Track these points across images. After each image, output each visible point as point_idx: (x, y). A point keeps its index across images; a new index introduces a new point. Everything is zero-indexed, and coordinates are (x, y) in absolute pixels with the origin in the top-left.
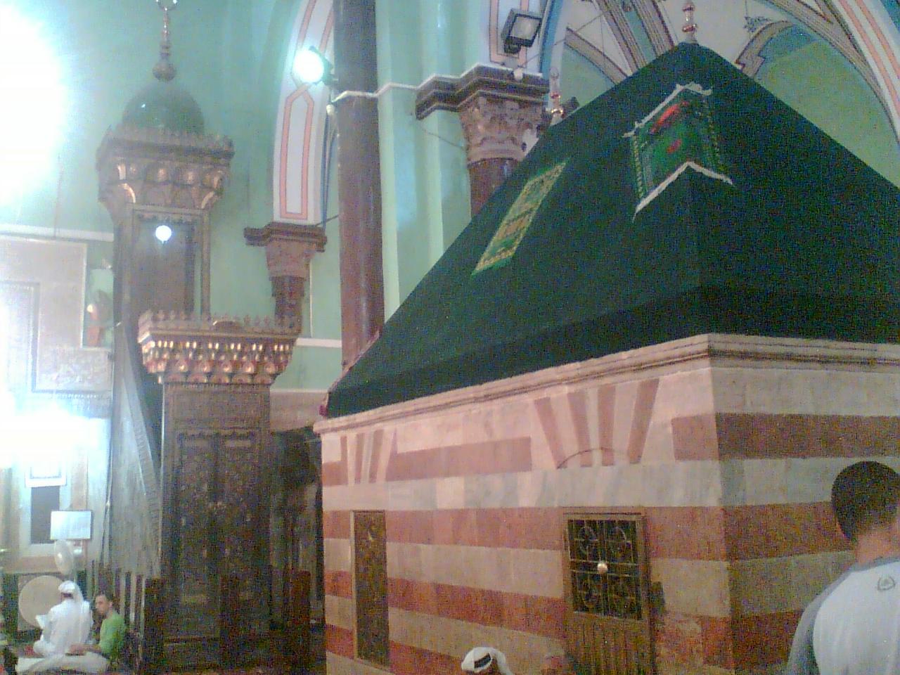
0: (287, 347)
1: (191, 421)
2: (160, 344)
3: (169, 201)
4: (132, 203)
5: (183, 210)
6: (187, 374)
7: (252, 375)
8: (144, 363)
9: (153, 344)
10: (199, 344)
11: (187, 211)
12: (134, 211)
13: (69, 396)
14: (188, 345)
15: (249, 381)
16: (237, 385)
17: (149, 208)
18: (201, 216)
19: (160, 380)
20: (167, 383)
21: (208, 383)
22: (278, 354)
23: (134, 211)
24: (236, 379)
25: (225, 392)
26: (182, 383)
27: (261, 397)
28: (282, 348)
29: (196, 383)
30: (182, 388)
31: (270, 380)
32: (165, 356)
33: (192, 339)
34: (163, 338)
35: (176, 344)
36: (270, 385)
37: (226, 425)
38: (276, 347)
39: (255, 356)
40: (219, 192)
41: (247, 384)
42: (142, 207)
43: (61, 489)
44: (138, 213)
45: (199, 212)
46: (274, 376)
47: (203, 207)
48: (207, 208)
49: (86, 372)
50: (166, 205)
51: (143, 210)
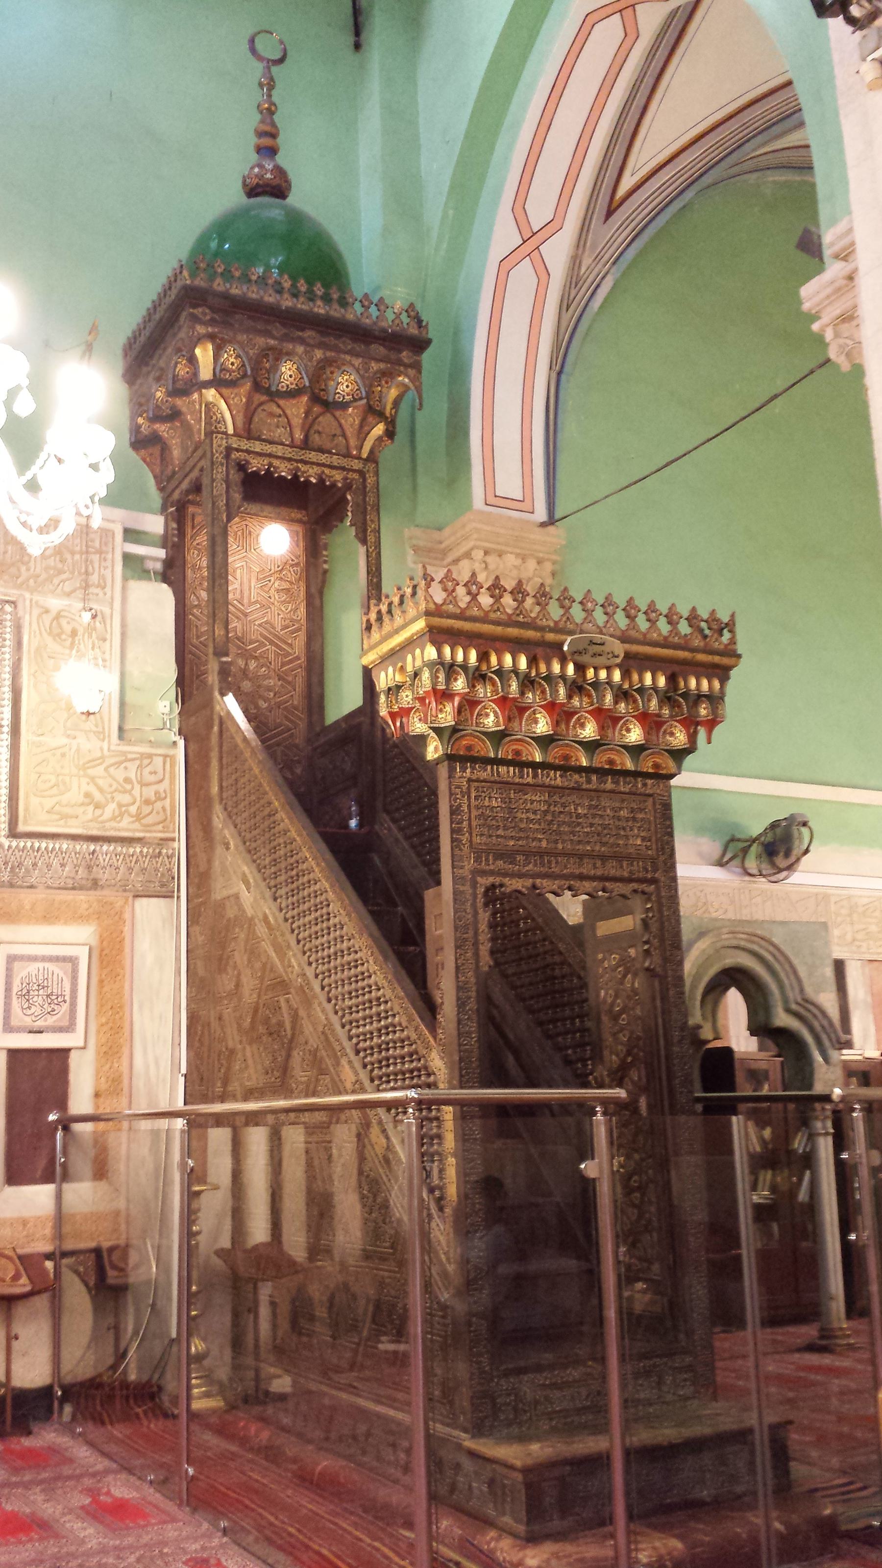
0: (717, 684)
1: (508, 855)
2: (447, 650)
3: (299, 435)
4: (225, 433)
5: (323, 458)
6: (498, 737)
7: (636, 751)
8: (383, 712)
9: (431, 652)
10: (533, 661)
11: (336, 460)
12: (229, 450)
13: (92, 847)
14: (508, 660)
15: (629, 765)
16: (601, 773)
17: (258, 447)
18: (361, 473)
19: (433, 750)
20: (450, 758)
21: (543, 765)
22: (700, 697)
23: (229, 450)
24: (600, 760)
25: (577, 789)
26: (487, 761)
27: (654, 804)
28: (705, 684)
29: (519, 763)
30: (486, 773)
31: (671, 765)
32: (460, 684)
33: (516, 645)
34: (454, 637)
35: (483, 657)
36: (672, 776)
37: (587, 869)
38: (693, 683)
39: (649, 700)
40: (390, 434)
41: (626, 773)
42: (245, 444)
43: (73, 1055)
44: (235, 455)
45: (356, 465)
46: (679, 755)
47: (365, 455)
48: (372, 458)
49: (126, 799)
50: (292, 446)
51: (248, 452)
